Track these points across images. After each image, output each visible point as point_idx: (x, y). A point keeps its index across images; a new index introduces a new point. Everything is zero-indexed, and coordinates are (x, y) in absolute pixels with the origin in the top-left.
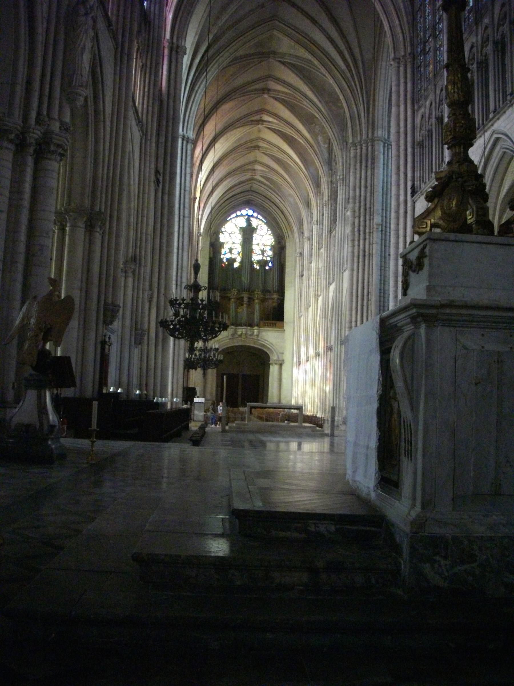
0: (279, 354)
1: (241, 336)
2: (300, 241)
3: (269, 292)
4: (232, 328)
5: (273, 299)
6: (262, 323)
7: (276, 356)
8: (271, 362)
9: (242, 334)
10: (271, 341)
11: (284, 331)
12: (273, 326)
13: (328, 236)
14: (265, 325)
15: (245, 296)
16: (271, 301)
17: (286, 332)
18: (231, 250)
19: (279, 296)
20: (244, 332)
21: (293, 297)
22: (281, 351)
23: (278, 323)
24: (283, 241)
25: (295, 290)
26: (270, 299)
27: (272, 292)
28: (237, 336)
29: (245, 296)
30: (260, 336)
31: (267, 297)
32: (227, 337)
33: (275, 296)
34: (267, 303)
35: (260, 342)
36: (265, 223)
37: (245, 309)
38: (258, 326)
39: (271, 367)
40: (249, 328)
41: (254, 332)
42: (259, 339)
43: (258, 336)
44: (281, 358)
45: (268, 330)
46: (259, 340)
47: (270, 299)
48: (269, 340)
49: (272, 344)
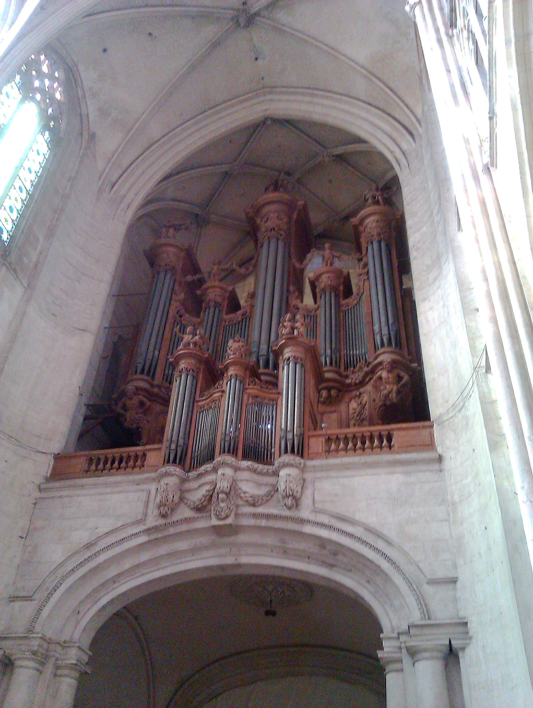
0: (428, 590)
7: (411, 600)
10: (372, 521)
11: (440, 459)
17: (447, 464)
20: (223, 485)
22: (441, 574)
30: (306, 501)
35: (308, 529)
39: (391, 679)
40: (245, 464)
42: (305, 513)
43: (297, 502)
45: (347, 467)
46: (302, 521)
48: (358, 517)
49: (379, 535)
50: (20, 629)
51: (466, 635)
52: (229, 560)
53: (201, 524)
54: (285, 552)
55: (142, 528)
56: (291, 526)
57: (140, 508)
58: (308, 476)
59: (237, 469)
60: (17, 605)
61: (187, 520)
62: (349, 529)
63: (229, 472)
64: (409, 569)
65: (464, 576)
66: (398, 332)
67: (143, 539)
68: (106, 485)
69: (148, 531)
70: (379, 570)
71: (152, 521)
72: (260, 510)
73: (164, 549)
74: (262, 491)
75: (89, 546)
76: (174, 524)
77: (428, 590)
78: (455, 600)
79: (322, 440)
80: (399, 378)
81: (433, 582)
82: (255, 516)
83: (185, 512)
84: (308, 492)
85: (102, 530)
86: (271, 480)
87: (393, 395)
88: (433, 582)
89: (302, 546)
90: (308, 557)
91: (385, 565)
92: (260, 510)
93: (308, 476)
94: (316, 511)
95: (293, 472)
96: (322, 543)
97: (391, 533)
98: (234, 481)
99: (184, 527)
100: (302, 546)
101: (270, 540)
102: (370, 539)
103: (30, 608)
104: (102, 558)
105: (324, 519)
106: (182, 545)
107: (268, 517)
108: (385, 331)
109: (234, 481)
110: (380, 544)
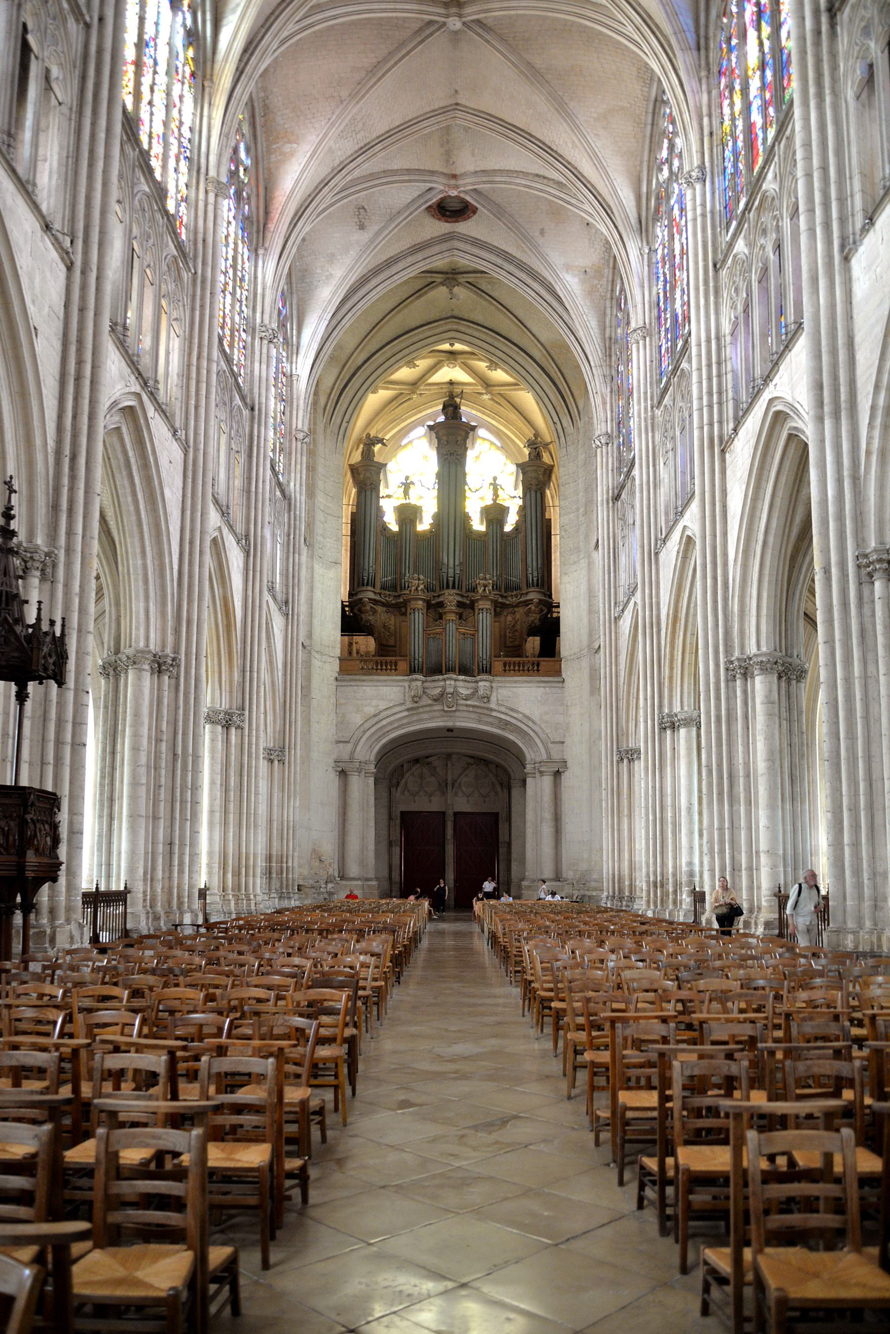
1: (437, 699)
2: (604, 403)
3: (518, 588)
4: (416, 680)
5: (527, 603)
6: (498, 666)
8: (529, 768)
9: (442, 694)
10: (527, 712)
12: (532, 669)
13: (818, 32)
14: (509, 669)
15: (451, 598)
16: (521, 610)
17: (566, 684)
18: (407, 486)
19: (545, 595)
21: (584, 588)
23: (545, 663)
24: (546, 458)
25: (590, 565)
26: (518, 605)
27: (524, 585)
28: (430, 702)
29: (451, 598)
30: (493, 699)
31: (511, 600)
32: (401, 704)
33: (534, 596)
34: (509, 618)
35: (494, 714)
36: (498, 448)
37: (452, 627)
38: (487, 670)
41: (476, 690)
42: (493, 705)
43: (488, 698)
44: (556, 756)
45: (515, 682)
46: (492, 710)
47: (518, 605)
50: (346, 757)
51: (566, 767)
52: (450, 724)
53: (436, 708)
54: (479, 721)
55: (403, 708)
56: (485, 712)
57: (402, 697)
58: (494, 685)
59: (456, 680)
60: (341, 745)
61: (429, 705)
62: (515, 715)
63: (453, 682)
64: (543, 736)
65: (568, 741)
66: (543, 577)
67: (406, 713)
68: (378, 681)
69: (408, 710)
70: (526, 733)
71: (409, 705)
72: (469, 702)
73: (415, 718)
74: (468, 692)
75: (375, 716)
76: (423, 707)
77: (551, 746)
78: (563, 751)
79: (501, 663)
80: (542, 610)
81: (553, 743)
82: (467, 705)
83: (426, 701)
84: (494, 694)
85: (382, 707)
86: (474, 685)
87: (537, 621)
88: (553, 743)
89: (490, 720)
90: (491, 724)
91: (532, 734)
92: (469, 702)
93: (494, 685)
94: (498, 704)
95: (487, 684)
96: (501, 720)
97: (536, 720)
98: (455, 687)
99: (428, 709)
100: (490, 720)
101: (473, 716)
102: (525, 720)
103: (350, 747)
104: (384, 722)
105: (503, 709)
106: (425, 716)
107: (474, 706)
108: (535, 574)
109: (455, 687)
110: (530, 724)
